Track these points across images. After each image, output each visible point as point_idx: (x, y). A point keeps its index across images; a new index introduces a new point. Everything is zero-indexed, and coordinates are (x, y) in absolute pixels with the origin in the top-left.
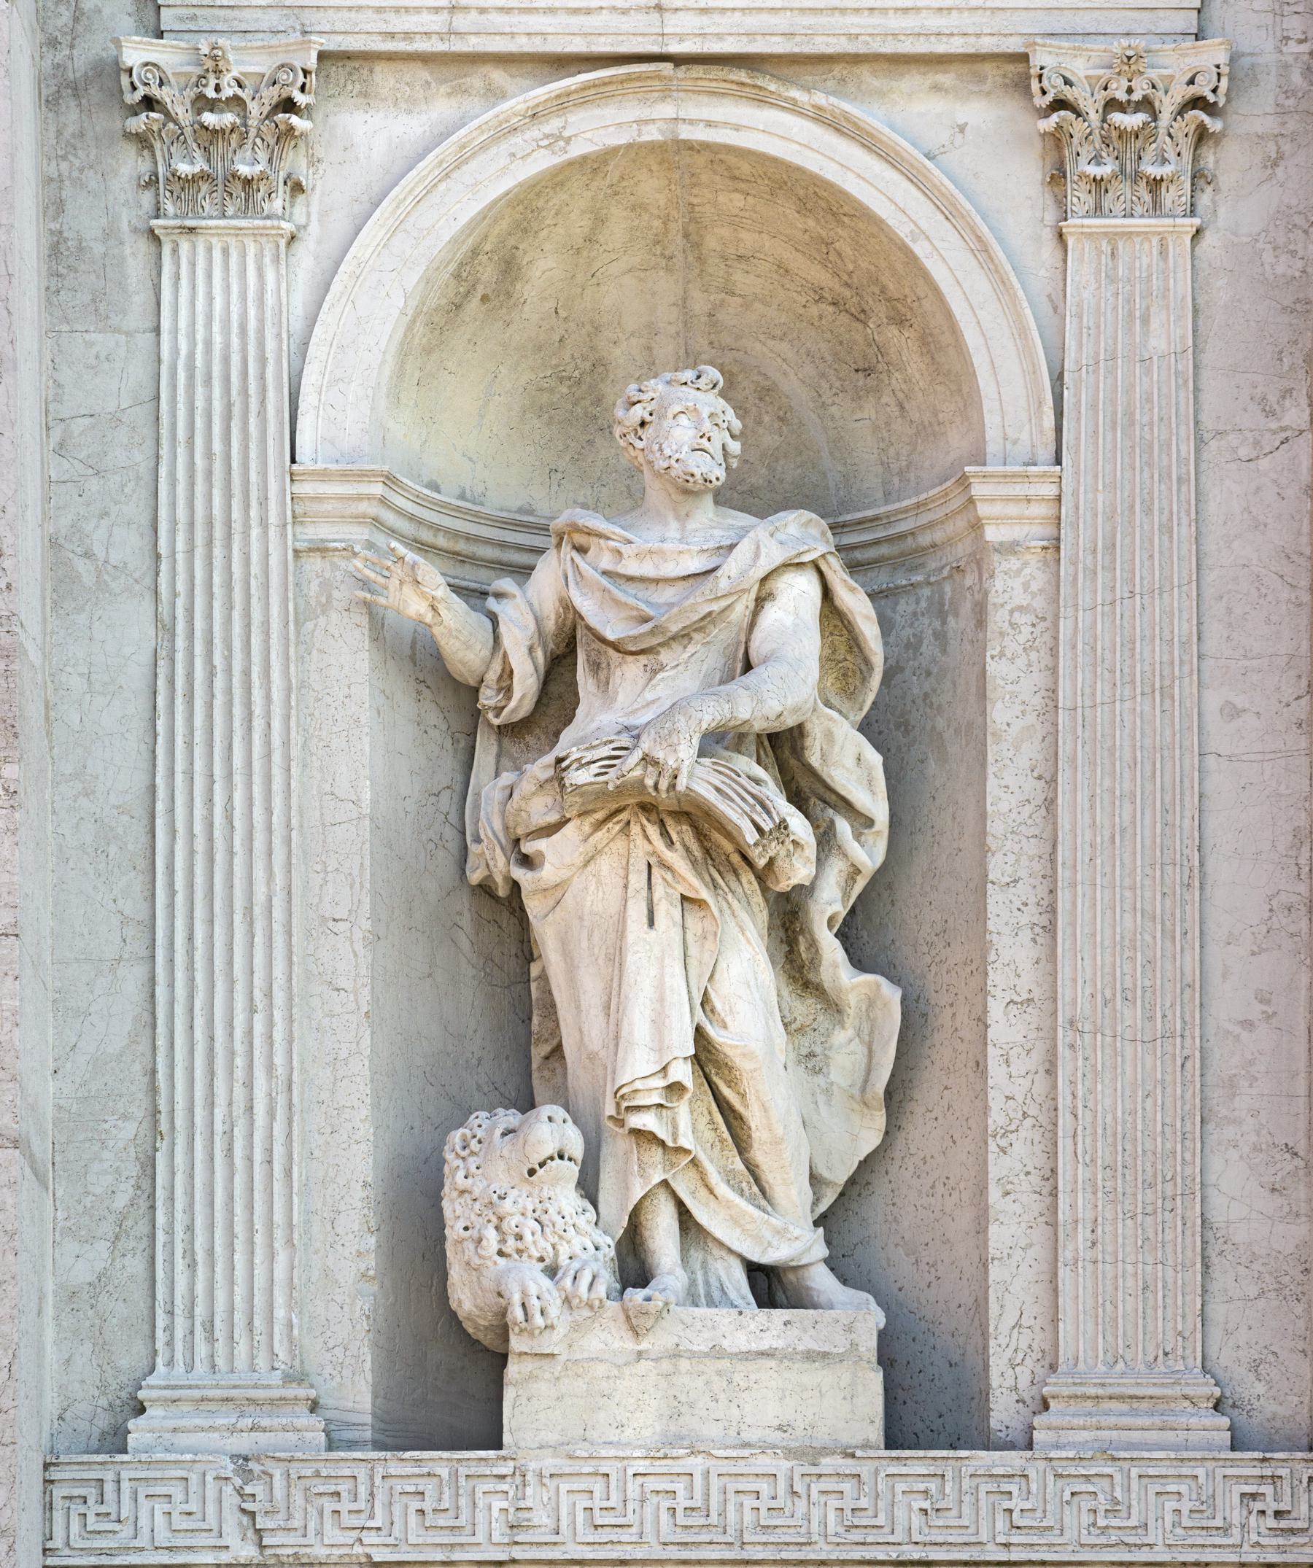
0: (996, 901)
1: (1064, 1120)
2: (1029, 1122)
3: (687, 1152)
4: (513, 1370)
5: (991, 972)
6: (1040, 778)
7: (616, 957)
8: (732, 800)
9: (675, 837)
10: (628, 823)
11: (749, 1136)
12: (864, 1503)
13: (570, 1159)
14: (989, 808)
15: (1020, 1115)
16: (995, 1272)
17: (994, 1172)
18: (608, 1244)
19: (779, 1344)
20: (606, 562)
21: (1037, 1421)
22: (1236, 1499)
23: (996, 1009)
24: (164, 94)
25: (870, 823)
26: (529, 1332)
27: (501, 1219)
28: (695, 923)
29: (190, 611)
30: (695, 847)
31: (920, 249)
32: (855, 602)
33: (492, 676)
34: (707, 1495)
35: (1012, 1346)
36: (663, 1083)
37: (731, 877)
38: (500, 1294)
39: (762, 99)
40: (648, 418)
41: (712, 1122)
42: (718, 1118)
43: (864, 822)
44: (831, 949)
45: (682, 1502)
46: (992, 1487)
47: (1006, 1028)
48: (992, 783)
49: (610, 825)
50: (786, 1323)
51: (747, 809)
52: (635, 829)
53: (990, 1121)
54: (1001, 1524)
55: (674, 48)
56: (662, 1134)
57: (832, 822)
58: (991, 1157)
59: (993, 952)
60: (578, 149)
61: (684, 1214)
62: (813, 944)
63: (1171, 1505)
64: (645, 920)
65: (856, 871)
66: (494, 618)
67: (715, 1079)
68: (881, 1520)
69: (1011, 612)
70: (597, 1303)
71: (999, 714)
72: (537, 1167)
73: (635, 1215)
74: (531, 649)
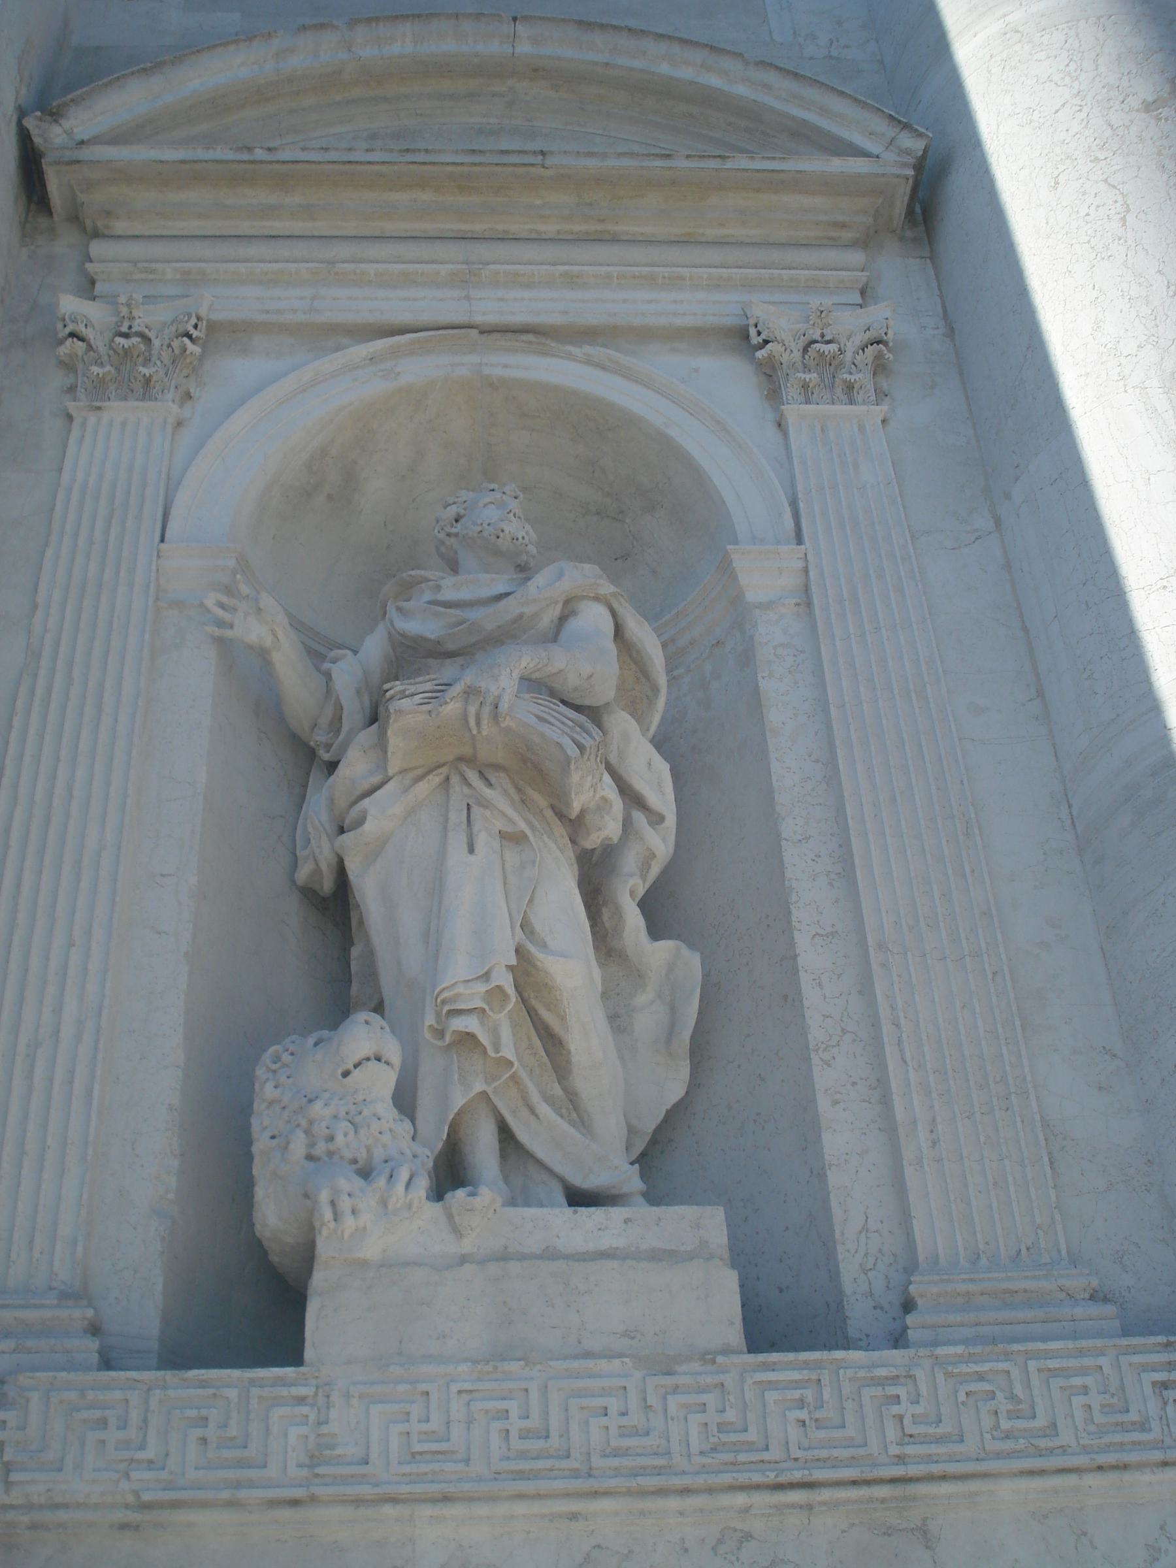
0: (790, 854)
1: (886, 1029)
5: (794, 911)
6: (817, 761)
7: (436, 889)
8: (550, 723)
9: (493, 781)
10: (448, 779)
11: (569, 1062)
12: (731, 1415)
14: (775, 784)
16: (834, 1179)
18: (427, 1155)
19: (620, 1242)
20: (427, 596)
21: (910, 1319)
22: (1148, 1389)
23: (802, 940)
24: (89, 333)
25: (661, 819)
27: (311, 1123)
28: (513, 857)
29: (57, 643)
30: (512, 791)
31: (673, 432)
32: (641, 632)
33: (324, 721)
34: (545, 1413)
38: (307, 1196)
40: (462, 512)
41: (531, 1046)
42: (537, 1043)
43: (657, 819)
44: (634, 919)
45: (516, 1424)
46: (877, 1391)
47: (812, 956)
48: (775, 767)
49: (430, 777)
52: (455, 779)
53: (810, 1037)
54: (892, 1433)
58: (815, 1070)
59: (794, 894)
62: (618, 913)
63: (1078, 1401)
64: (465, 847)
66: (328, 676)
67: (533, 1002)
68: (752, 1435)
69: (775, 648)
71: (775, 716)
73: (454, 1128)
74: (358, 692)
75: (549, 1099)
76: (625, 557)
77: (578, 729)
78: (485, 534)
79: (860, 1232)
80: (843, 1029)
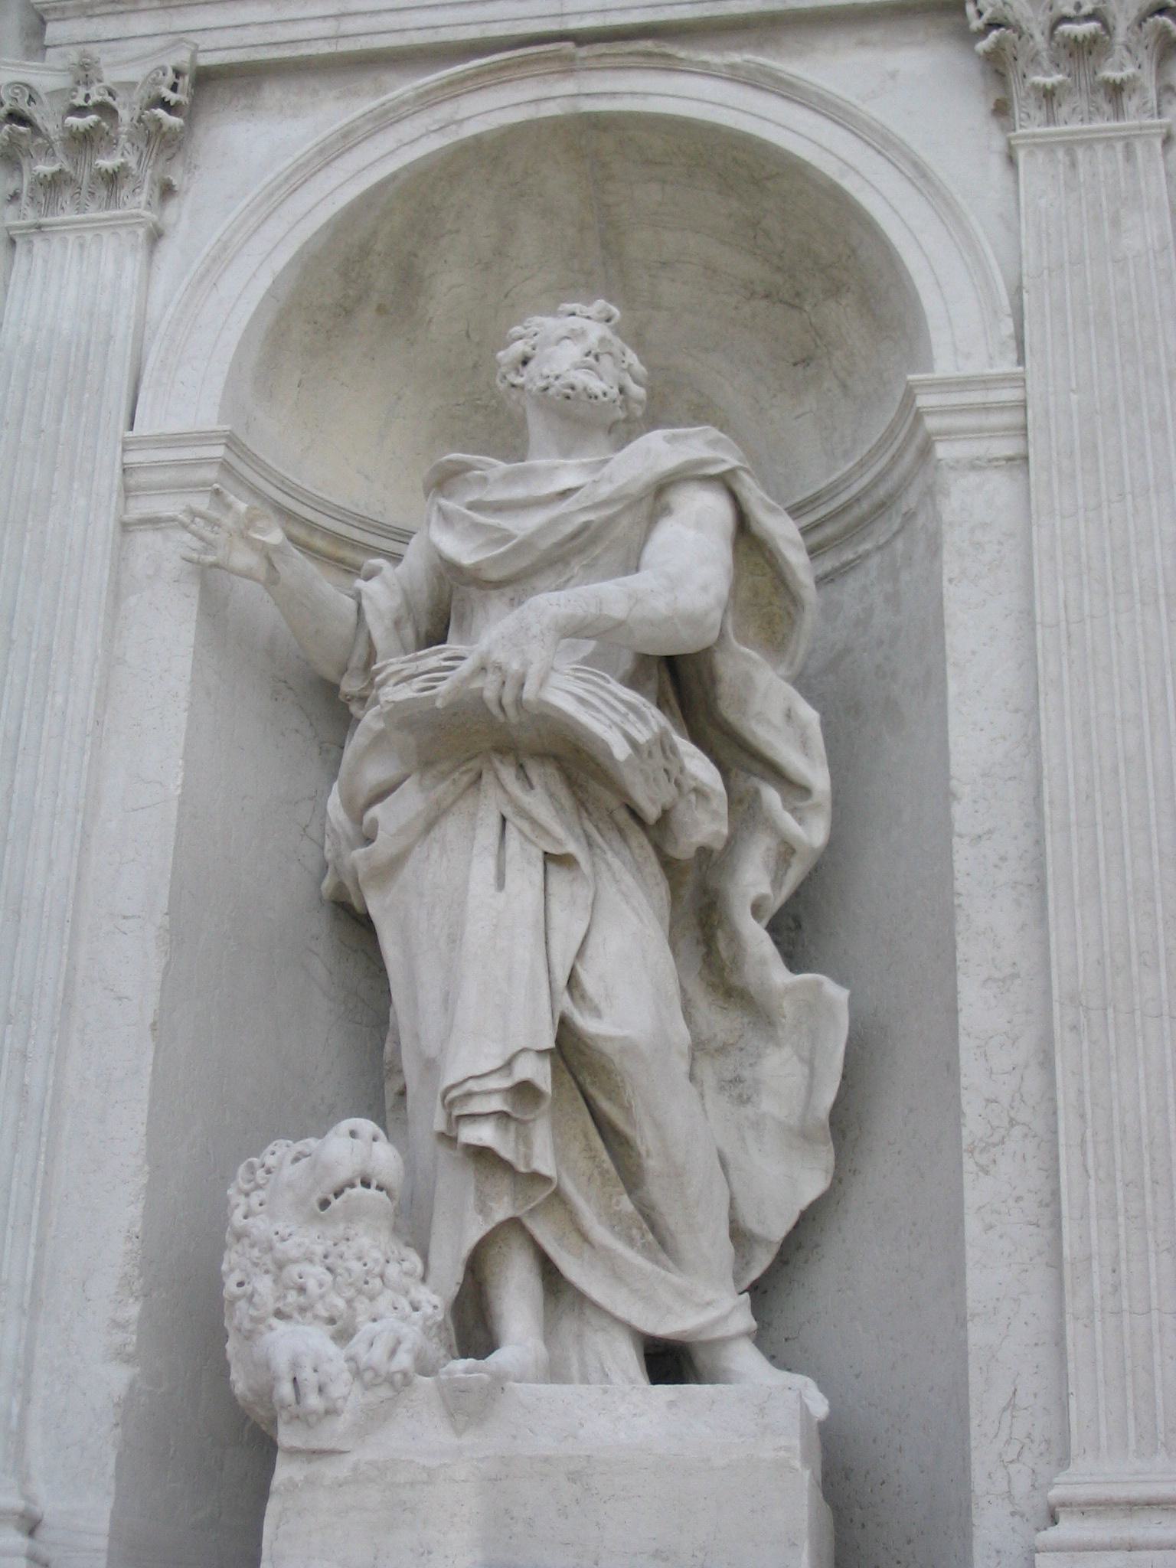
2: (1017, 1131)
3: (546, 1180)
4: (284, 1472)
9: (535, 780)
11: (640, 1166)
13: (380, 1188)
15: (1006, 1123)
16: (977, 1335)
17: (972, 1197)
20: (473, 496)
25: (805, 791)
26: (304, 1419)
31: (849, 184)
35: (1004, 1436)
36: (507, 1083)
37: (613, 835)
39: (670, 66)
41: (589, 1148)
42: (598, 1142)
49: (456, 775)
50: (671, 1404)
51: (617, 718)
52: (487, 778)
53: (965, 1132)
55: (574, 24)
56: (506, 1152)
57: (757, 792)
58: (967, 1179)
60: (470, 130)
61: (550, 1274)
62: (735, 937)
64: (492, 880)
65: (787, 851)
70: (398, 1377)
72: (331, 1197)
74: (397, 624)
75: (614, 1221)
76: (805, 361)
77: (631, 716)
78: (551, 391)
79: (1005, 1409)
80: (1011, 1120)
